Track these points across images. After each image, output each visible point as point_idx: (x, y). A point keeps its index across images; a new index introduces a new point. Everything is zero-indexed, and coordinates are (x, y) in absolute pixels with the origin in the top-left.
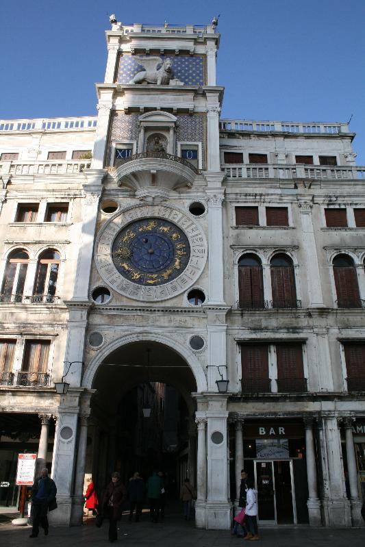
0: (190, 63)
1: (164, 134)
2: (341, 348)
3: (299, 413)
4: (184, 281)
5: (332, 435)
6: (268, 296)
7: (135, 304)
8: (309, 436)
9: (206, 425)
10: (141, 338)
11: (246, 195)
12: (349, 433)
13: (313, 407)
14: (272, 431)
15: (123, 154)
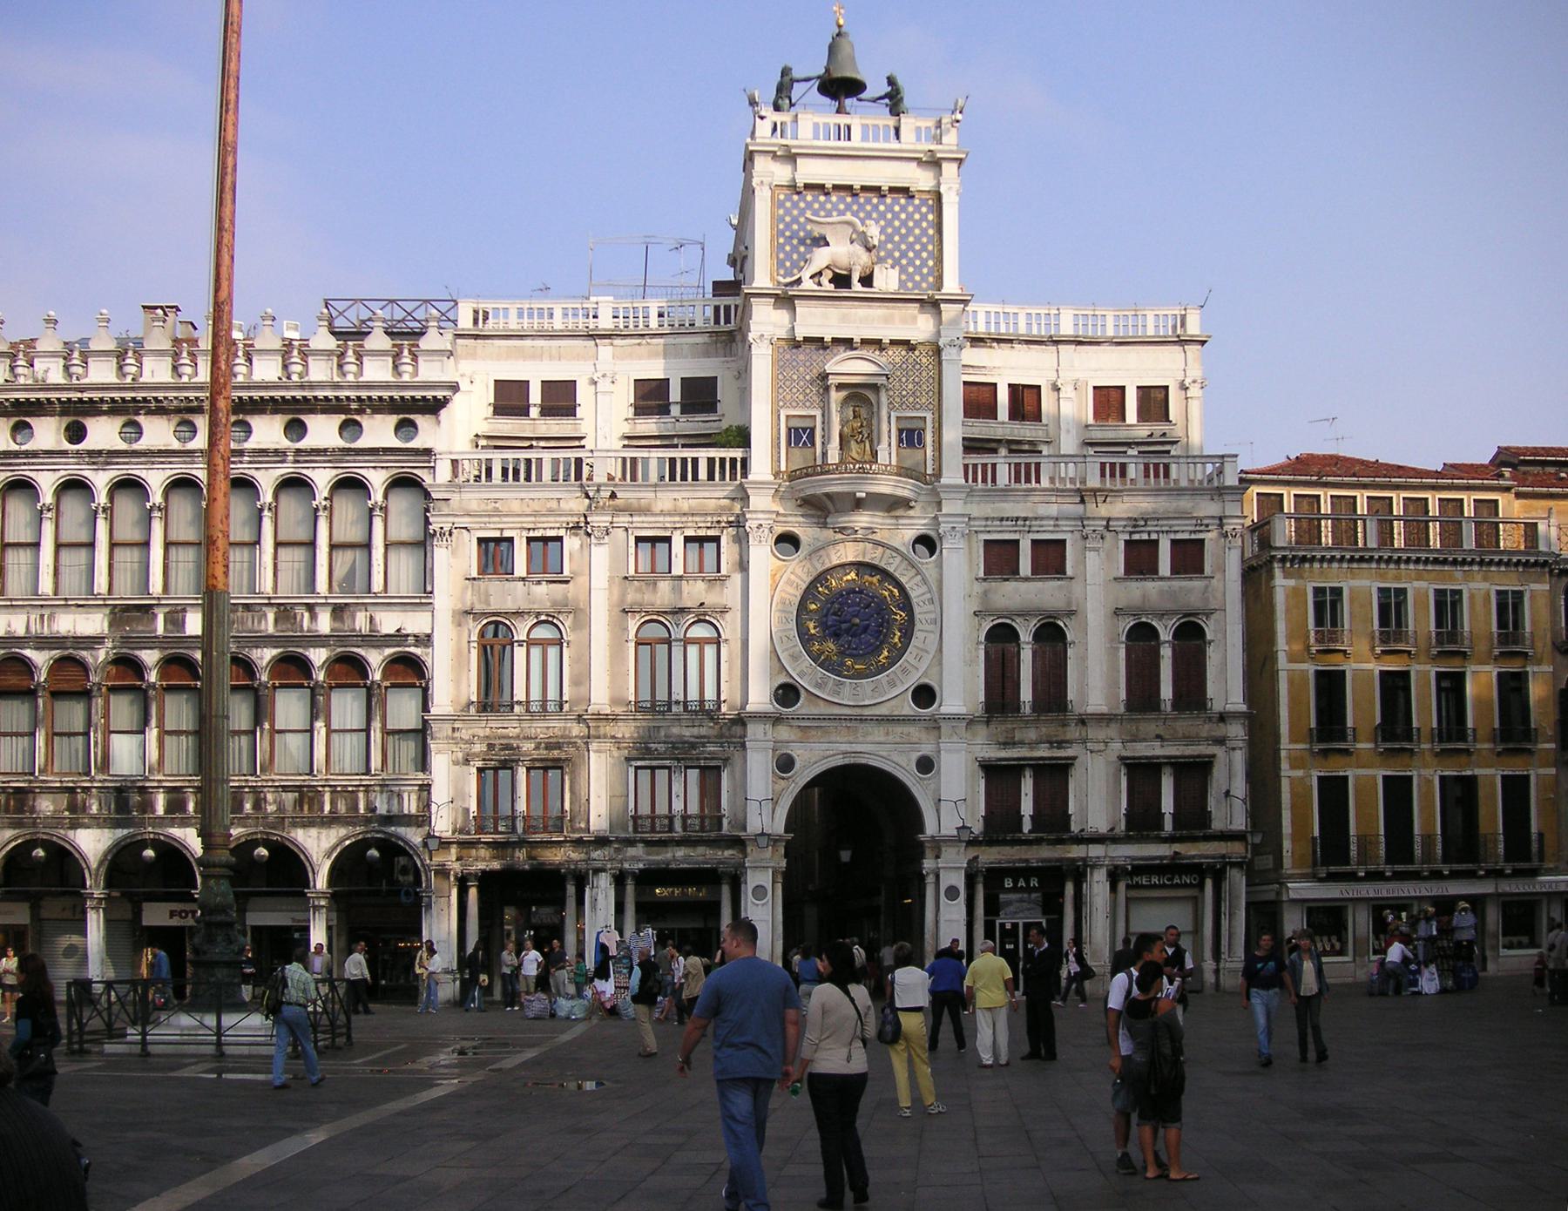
0: (910, 216)
1: (871, 395)
2: (1123, 771)
3: (1058, 860)
4: (904, 671)
5: (1098, 887)
6: (1026, 694)
7: (836, 710)
8: (1069, 889)
9: (938, 877)
10: (846, 761)
11: (1002, 519)
12: (1122, 886)
13: (1076, 852)
14: (1022, 883)
15: (798, 438)
